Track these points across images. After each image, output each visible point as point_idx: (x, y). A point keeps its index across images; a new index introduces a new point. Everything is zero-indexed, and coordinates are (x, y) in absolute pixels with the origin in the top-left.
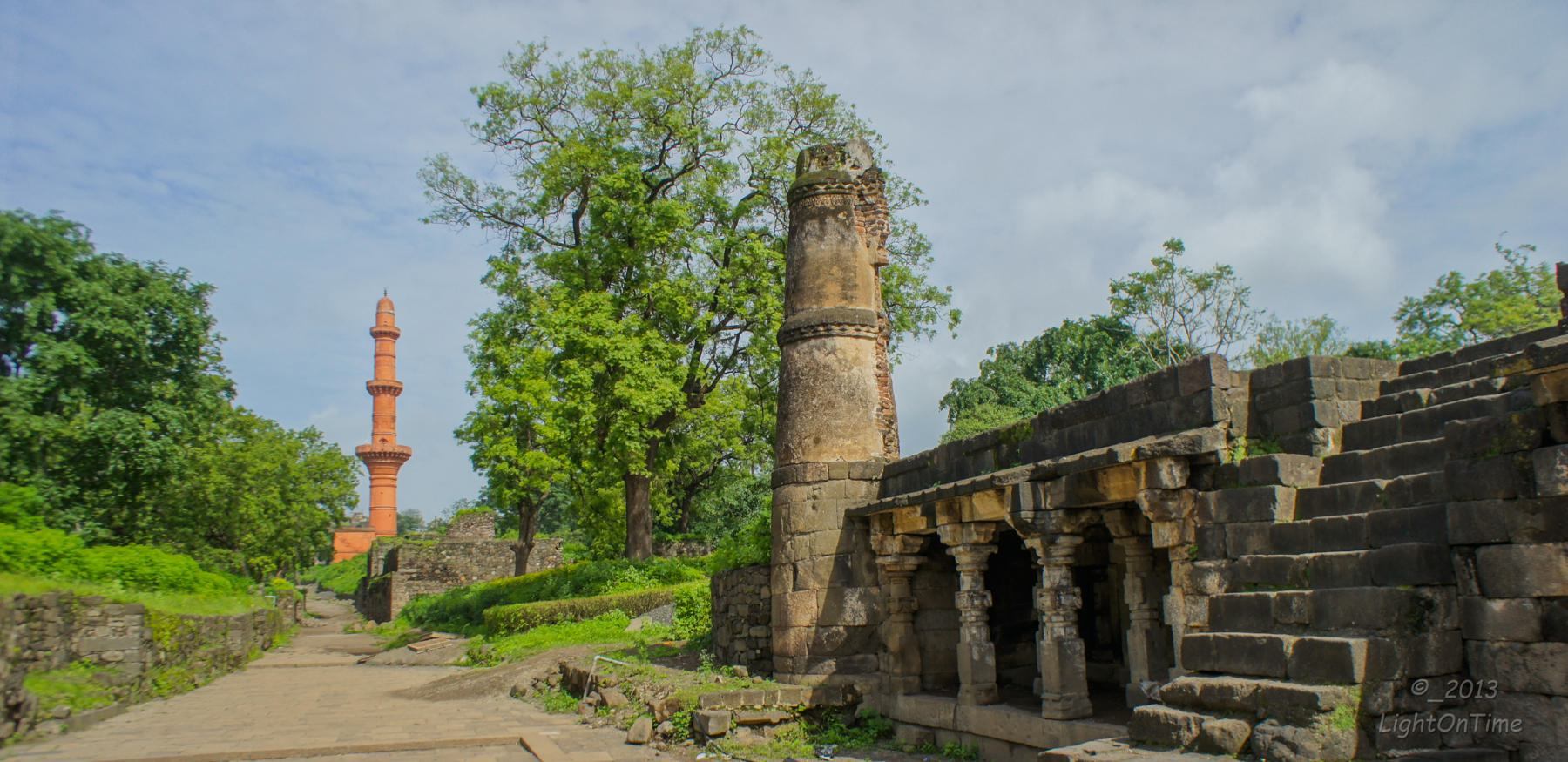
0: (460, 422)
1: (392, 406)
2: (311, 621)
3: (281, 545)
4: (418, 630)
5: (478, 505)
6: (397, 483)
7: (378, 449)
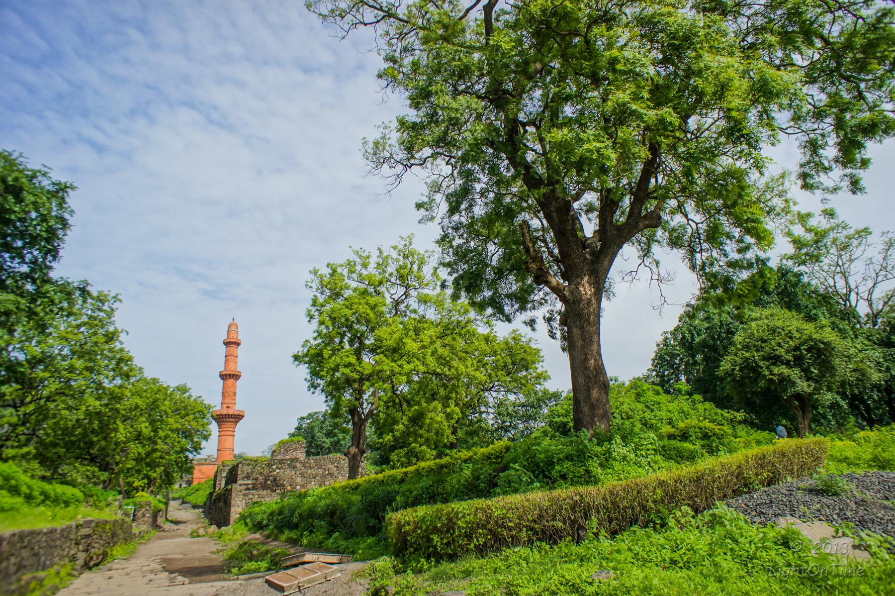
0: (299, 350)
1: (234, 386)
2: (168, 526)
3: (148, 465)
4: (257, 535)
5: (293, 435)
6: (235, 434)
7: (225, 412)
